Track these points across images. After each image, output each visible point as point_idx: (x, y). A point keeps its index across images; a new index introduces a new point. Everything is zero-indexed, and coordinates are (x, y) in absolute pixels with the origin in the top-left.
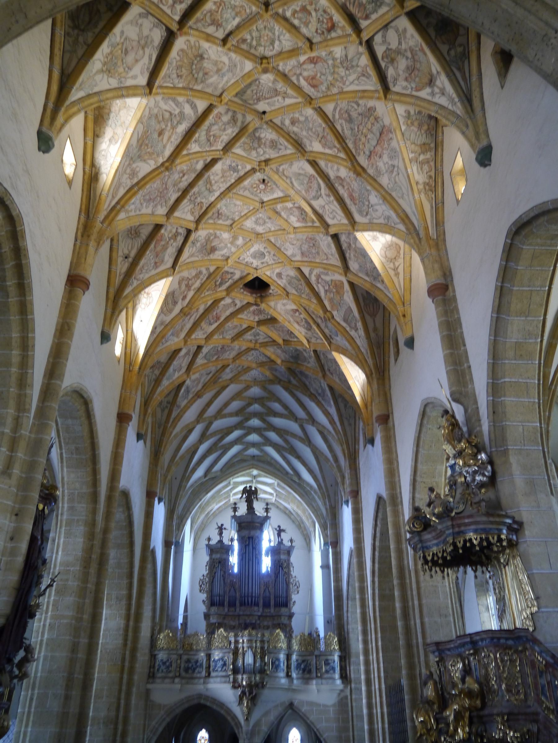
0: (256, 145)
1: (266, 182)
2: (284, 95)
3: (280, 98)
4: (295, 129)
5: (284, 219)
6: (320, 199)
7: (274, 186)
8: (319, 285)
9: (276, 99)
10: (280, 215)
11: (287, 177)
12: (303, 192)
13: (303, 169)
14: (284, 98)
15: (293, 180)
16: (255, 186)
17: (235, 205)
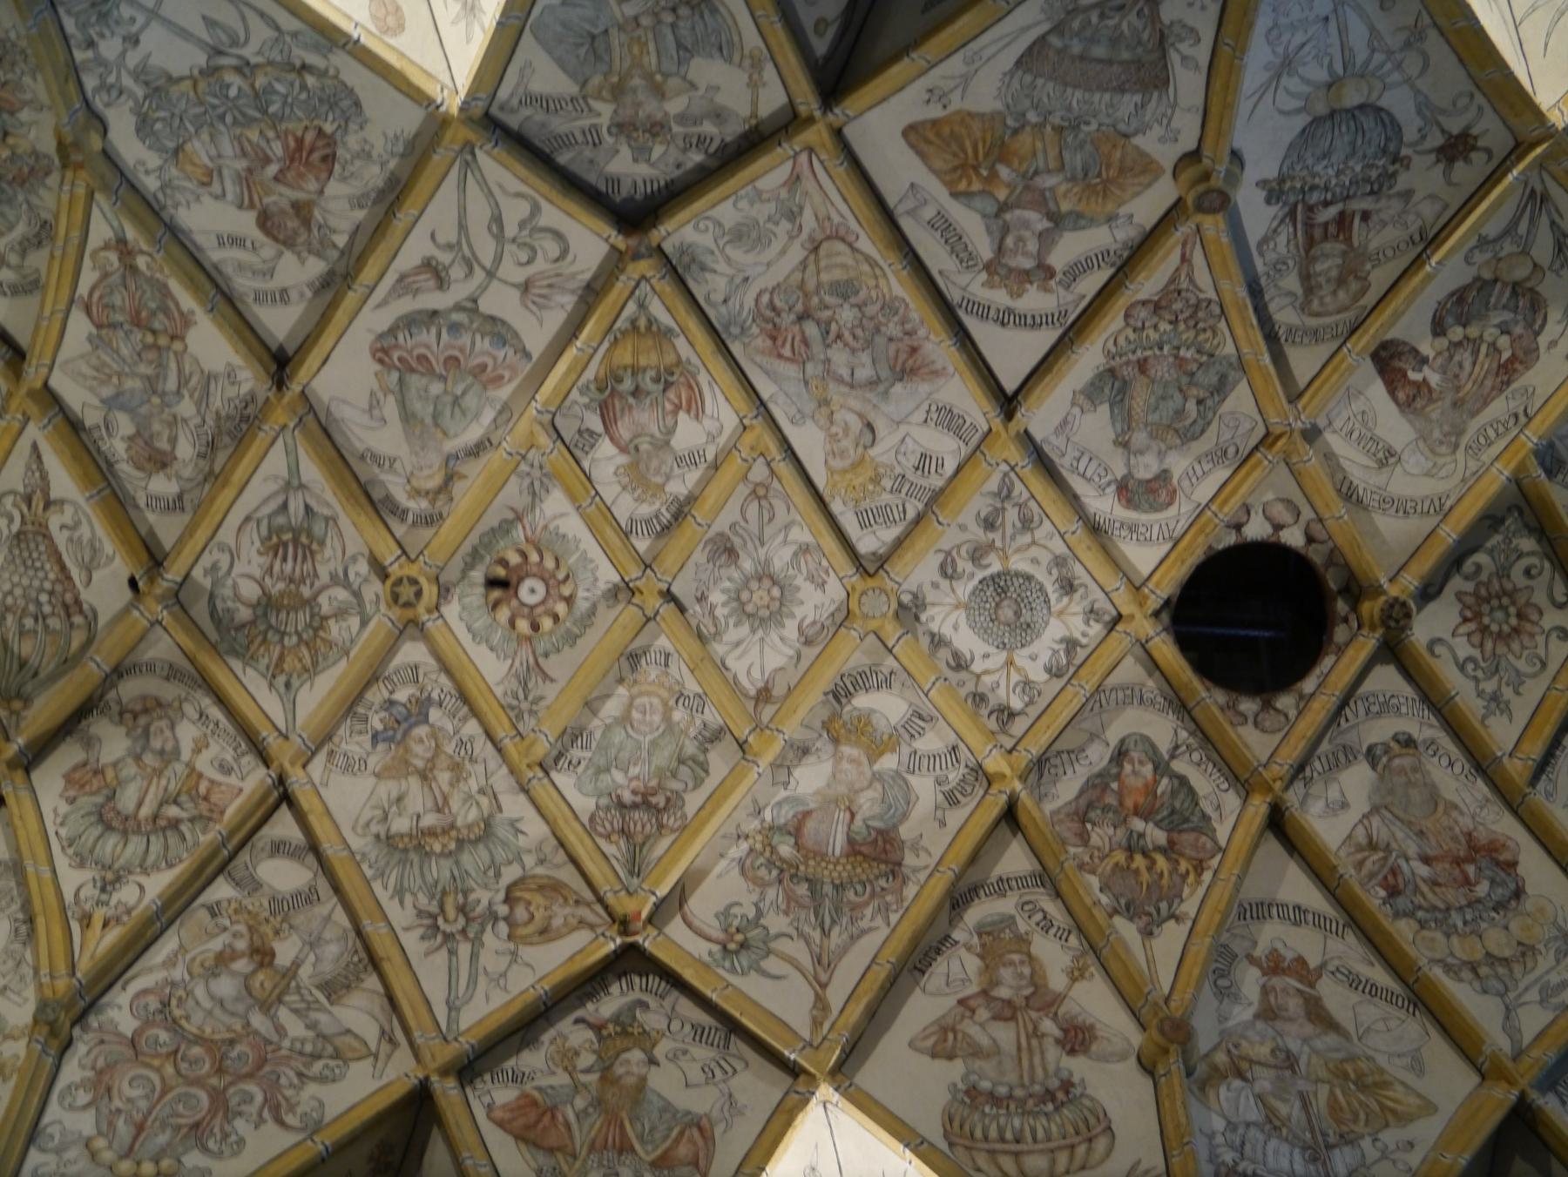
0: (302, 618)
1: (501, 572)
2: (38, 503)
3: (54, 521)
4: (185, 450)
5: (705, 483)
6: (485, 306)
7: (519, 534)
8: (1059, 258)
9: (60, 539)
10: (692, 499)
11: (450, 478)
12: (504, 392)
13: (374, 405)
14: (48, 504)
15: (450, 446)
16: (523, 625)
17: (625, 720)
